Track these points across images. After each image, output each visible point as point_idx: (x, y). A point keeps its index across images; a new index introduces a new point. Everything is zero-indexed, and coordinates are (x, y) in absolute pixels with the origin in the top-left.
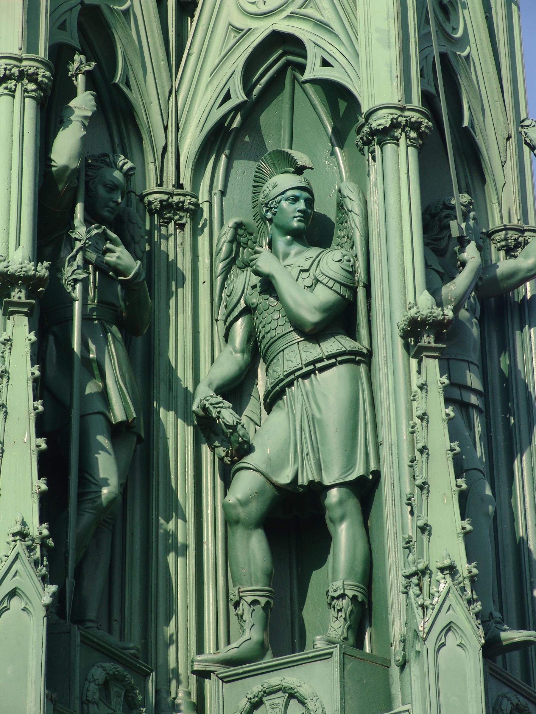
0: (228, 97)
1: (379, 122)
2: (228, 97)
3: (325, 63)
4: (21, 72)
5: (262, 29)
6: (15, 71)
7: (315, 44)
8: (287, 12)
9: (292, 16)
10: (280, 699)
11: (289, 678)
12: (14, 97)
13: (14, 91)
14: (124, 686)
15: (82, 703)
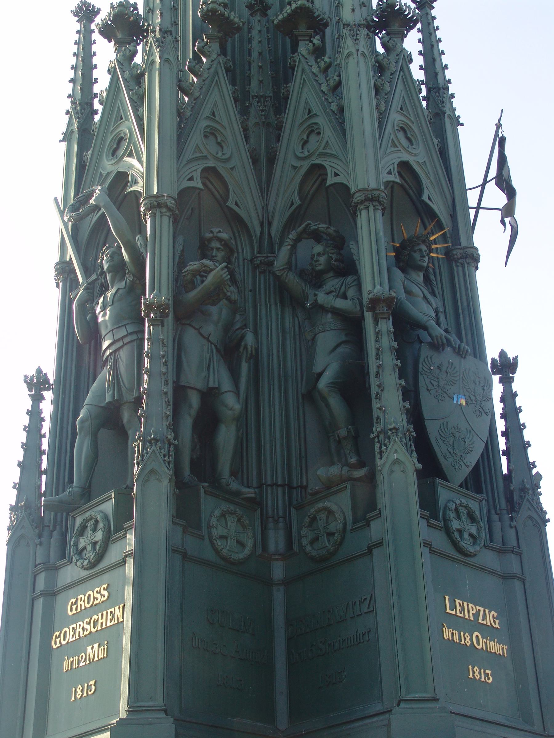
0: (292, 204)
1: (358, 199)
2: (292, 204)
3: (336, 175)
4: (158, 204)
5: (306, 165)
6: (155, 203)
7: (331, 166)
8: (317, 153)
9: (321, 155)
10: (323, 516)
11: (327, 504)
12: (155, 217)
13: (156, 214)
14: (237, 516)
15: (208, 528)
